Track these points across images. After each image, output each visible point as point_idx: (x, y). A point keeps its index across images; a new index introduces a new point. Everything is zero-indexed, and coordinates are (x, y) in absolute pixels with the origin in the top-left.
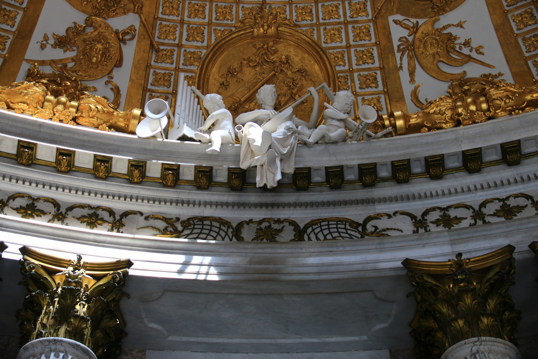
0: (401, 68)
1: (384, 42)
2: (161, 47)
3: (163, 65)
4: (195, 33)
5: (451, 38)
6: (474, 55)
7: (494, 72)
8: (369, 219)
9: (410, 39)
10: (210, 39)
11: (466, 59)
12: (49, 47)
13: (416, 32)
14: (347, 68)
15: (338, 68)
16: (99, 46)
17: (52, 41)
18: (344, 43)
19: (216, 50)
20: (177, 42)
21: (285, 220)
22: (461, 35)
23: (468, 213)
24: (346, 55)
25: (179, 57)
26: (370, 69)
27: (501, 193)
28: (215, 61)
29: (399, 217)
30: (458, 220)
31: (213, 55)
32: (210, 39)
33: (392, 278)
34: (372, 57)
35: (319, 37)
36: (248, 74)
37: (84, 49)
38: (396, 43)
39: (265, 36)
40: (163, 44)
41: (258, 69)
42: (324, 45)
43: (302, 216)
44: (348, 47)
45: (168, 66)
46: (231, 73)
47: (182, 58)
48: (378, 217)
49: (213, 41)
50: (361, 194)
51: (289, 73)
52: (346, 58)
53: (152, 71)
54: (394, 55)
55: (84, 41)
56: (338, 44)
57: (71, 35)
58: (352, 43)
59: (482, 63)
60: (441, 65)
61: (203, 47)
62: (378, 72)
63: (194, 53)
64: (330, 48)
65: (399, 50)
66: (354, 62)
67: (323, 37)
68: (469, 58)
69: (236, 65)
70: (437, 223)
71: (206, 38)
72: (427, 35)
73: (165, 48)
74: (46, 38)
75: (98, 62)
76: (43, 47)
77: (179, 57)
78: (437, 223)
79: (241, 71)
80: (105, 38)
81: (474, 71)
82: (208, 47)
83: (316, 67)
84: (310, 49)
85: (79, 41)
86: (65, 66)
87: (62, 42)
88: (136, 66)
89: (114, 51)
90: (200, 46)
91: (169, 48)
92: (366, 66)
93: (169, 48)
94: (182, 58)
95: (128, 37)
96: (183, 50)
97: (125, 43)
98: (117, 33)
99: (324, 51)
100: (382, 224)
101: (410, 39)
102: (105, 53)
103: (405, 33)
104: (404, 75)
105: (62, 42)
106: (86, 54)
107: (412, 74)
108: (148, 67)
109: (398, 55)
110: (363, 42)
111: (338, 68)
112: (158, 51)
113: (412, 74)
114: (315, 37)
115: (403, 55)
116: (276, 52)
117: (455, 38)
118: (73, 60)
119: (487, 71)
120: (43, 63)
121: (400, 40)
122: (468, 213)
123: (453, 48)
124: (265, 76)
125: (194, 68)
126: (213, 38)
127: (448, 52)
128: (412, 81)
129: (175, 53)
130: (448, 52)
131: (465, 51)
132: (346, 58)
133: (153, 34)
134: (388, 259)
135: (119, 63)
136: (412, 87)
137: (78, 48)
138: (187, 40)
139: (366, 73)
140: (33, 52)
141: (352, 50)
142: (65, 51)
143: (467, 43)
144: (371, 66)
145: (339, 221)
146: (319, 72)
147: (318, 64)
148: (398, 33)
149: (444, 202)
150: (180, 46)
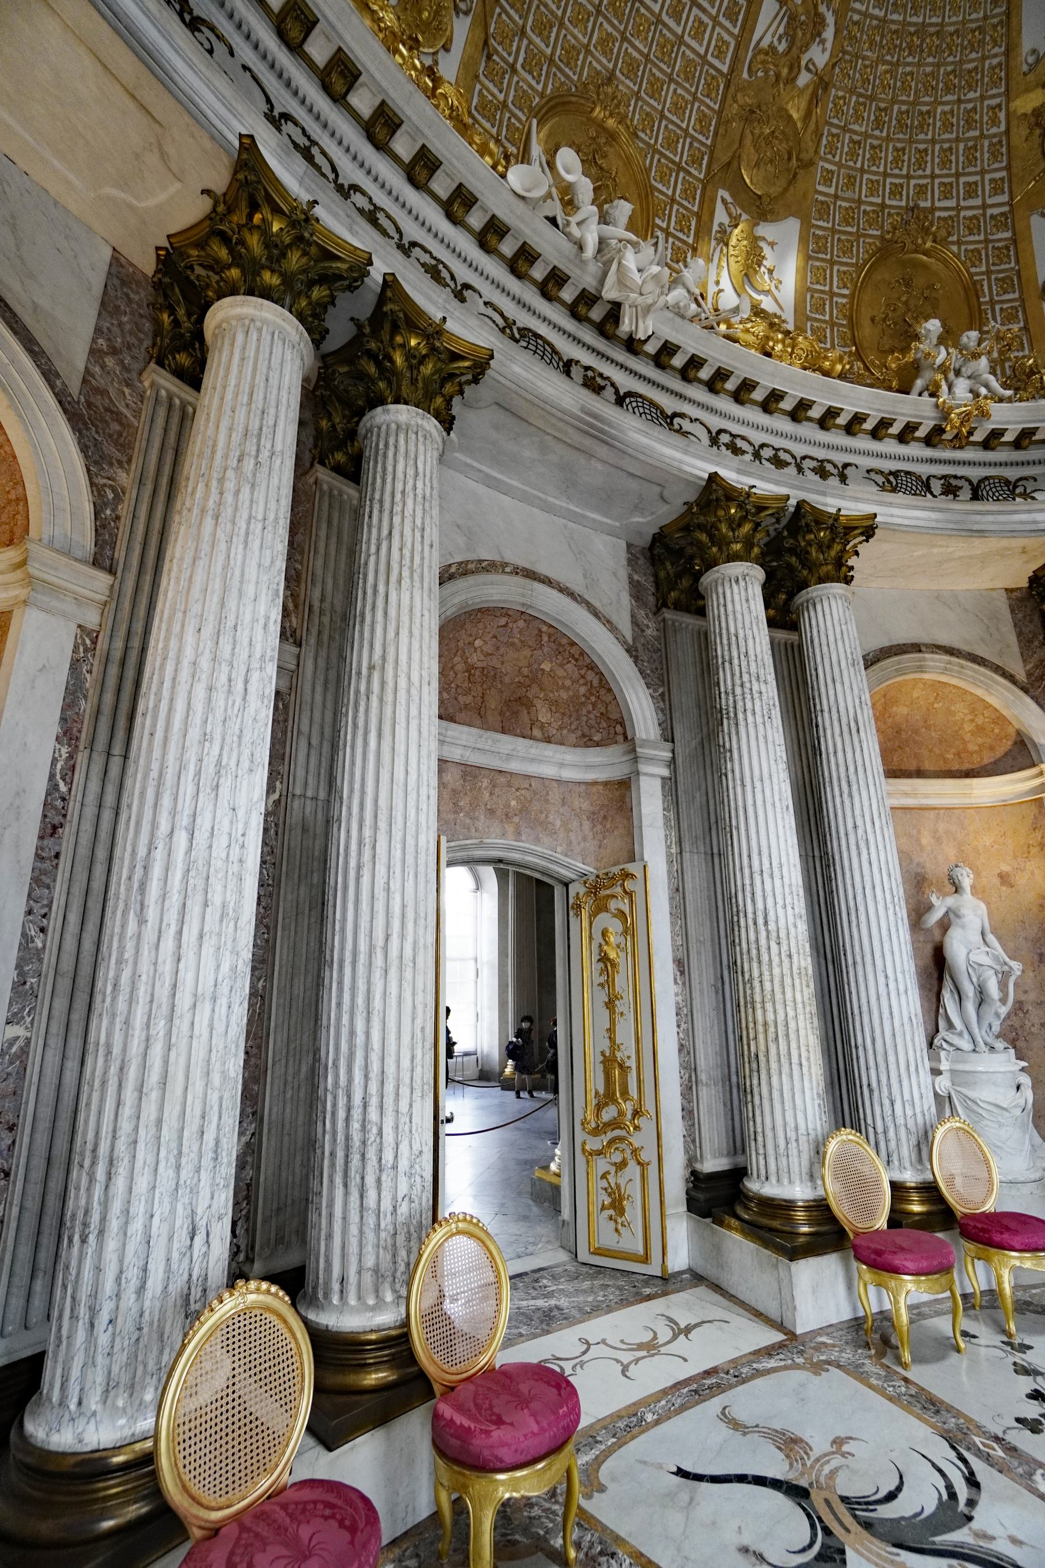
1: (705, 218)
8: (675, 415)
21: (608, 378)
23: (750, 449)
27: (778, 442)
29: (698, 424)
30: (744, 452)
33: (688, 482)
38: (715, 228)
39: (601, 126)
43: (625, 383)
48: (682, 415)
50: (677, 385)
70: (726, 445)
78: (726, 445)
81: (767, 304)
100: (687, 426)
103: (726, 220)
119: (779, 312)
122: (750, 449)
134: (699, 464)
136: (716, 289)
145: (652, 404)
149: (736, 429)
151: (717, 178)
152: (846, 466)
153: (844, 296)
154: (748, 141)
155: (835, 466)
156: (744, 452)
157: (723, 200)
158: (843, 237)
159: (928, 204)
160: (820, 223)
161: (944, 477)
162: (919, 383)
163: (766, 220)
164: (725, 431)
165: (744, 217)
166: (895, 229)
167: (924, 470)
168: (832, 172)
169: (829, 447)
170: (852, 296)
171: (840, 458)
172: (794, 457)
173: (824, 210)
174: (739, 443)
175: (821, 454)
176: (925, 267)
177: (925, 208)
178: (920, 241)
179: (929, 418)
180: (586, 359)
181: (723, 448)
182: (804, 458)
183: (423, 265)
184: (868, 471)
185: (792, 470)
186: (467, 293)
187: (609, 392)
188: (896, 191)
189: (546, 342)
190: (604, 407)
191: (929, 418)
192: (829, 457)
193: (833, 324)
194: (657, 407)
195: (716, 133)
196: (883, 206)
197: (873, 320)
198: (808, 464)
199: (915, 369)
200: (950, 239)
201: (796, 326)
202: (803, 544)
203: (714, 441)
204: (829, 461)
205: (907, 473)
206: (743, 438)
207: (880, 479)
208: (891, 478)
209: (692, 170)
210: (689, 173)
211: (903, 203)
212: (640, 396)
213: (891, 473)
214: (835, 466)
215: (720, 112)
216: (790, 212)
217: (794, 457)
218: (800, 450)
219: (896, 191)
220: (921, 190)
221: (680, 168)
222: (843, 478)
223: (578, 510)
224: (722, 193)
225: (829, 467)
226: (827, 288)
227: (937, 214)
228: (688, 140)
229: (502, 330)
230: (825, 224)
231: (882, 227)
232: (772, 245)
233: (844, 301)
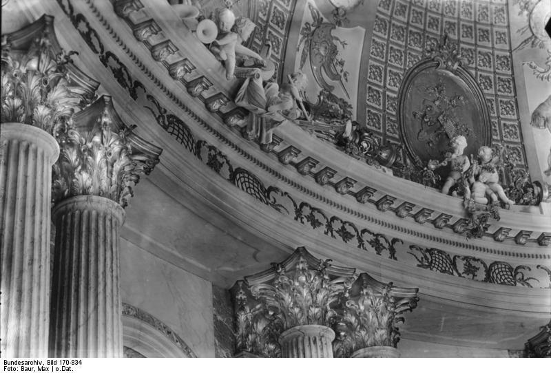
5: (334, 51)
8: (271, 189)
21: (224, 157)
23: (324, 222)
30: (320, 224)
48: (276, 190)
50: (274, 164)
81: (338, 93)
100: (281, 200)
119: (346, 99)
143: (342, 63)
152: (395, 240)
155: (387, 241)
156: (320, 224)
159: (456, 38)
160: (379, 34)
161: (466, 258)
162: (450, 182)
164: (306, 204)
167: (452, 250)
169: (383, 224)
171: (391, 234)
172: (356, 230)
174: (317, 216)
175: (376, 228)
178: (450, 64)
180: (211, 140)
181: (305, 220)
182: (364, 231)
183: (114, 71)
184: (411, 247)
185: (355, 241)
186: (139, 89)
187: (225, 170)
189: (185, 127)
190: (220, 182)
192: (382, 232)
194: (256, 180)
198: (367, 237)
199: (445, 173)
202: (362, 308)
203: (299, 212)
204: (382, 236)
205: (440, 252)
206: (319, 211)
207: (420, 255)
208: (428, 254)
212: (247, 172)
213: (427, 250)
214: (387, 241)
217: (356, 230)
218: (361, 224)
222: (392, 251)
223: (180, 256)
225: (382, 241)
227: (462, 45)
229: (158, 119)
231: (423, 46)
233: (396, 96)
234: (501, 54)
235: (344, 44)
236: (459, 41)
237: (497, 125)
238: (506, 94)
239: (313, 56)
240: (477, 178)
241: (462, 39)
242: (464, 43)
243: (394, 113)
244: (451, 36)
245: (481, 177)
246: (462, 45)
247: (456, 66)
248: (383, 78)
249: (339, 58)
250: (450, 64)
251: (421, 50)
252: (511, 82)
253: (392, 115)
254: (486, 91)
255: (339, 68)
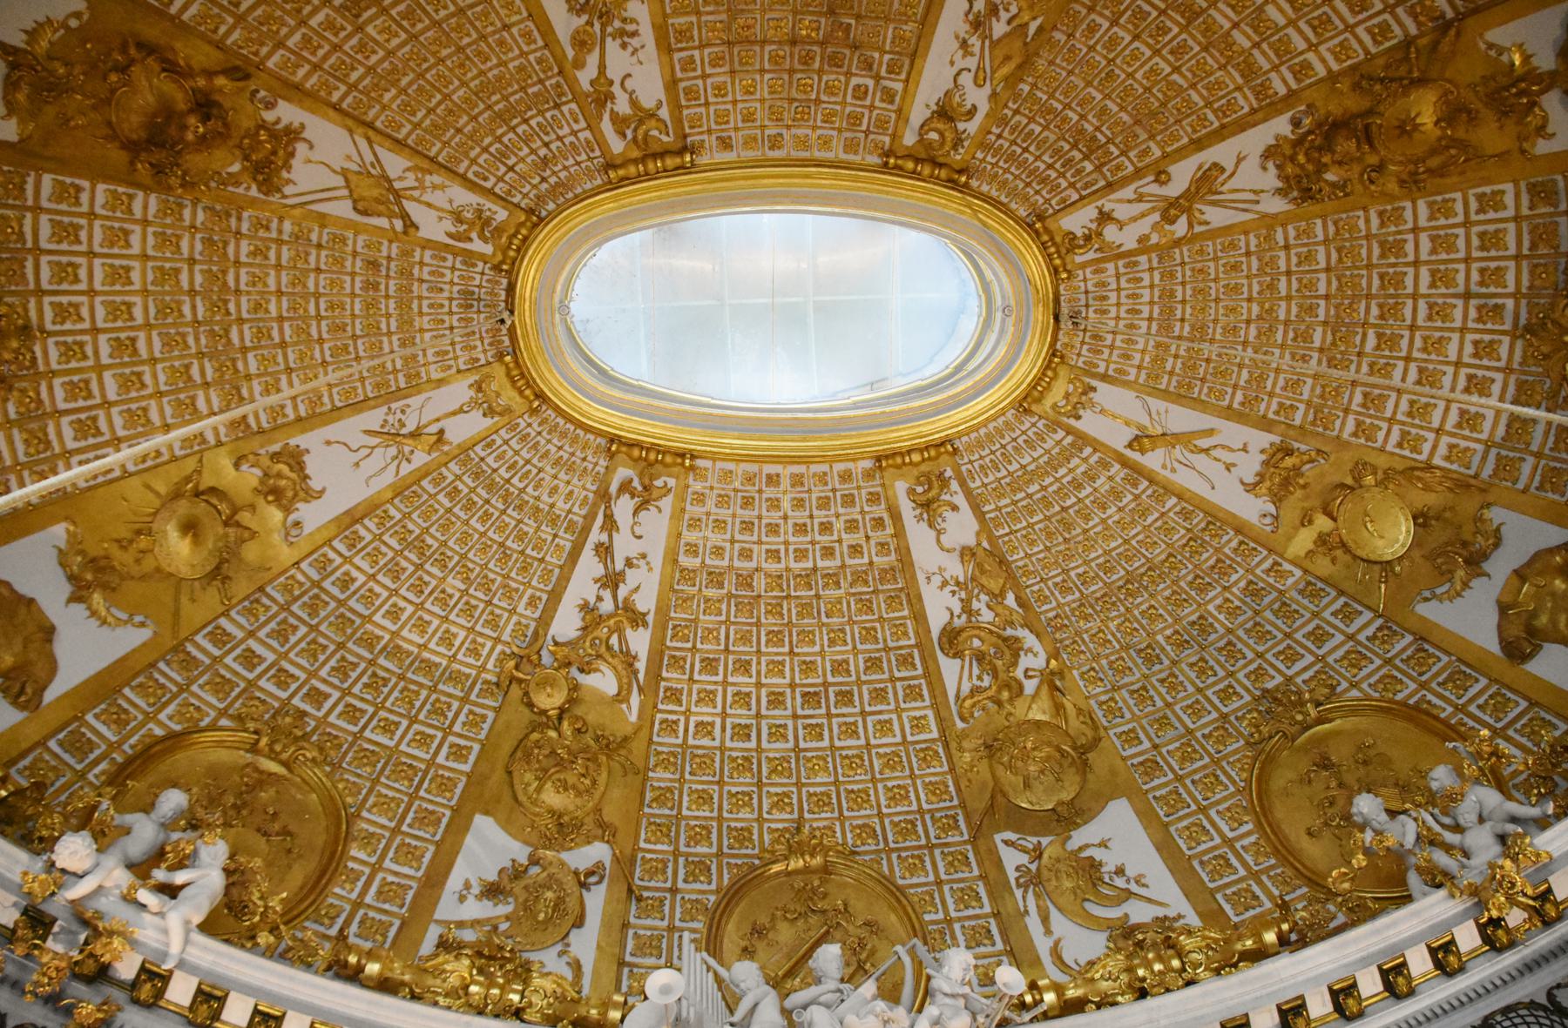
0: (1027, 912)
2: (645, 894)
3: (649, 922)
4: (699, 868)
5: (1094, 865)
6: (1134, 888)
7: (1172, 914)
9: (1033, 867)
10: (720, 876)
11: (1124, 895)
12: (471, 900)
13: (1040, 856)
14: (941, 916)
15: (927, 917)
16: (549, 895)
17: (476, 890)
18: (931, 878)
19: (732, 896)
20: (668, 885)
22: (1109, 860)
24: (936, 895)
25: (673, 908)
26: (977, 917)
28: (730, 917)
31: (728, 904)
32: (720, 876)
34: (978, 899)
35: (891, 869)
36: (785, 933)
37: (526, 900)
38: (1012, 875)
39: (807, 870)
40: (647, 889)
41: (800, 923)
42: (900, 882)
44: (939, 883)
45: (658, 923)
46: (758, 931)
47: (678, 910)
49: (726, 881)
51: (851, 928)
52: (938, 901)
53: (631, 932)
54: (1012, 894)
55: (526, 888)
56: (923, 880)
57: (506, 880)
58: (943, 877)
59: (1149, 900)
60: (1087, 905)
61: (711, 892)
62: (992, 921)
63: (697, 901)
64: (912, 886)
65: (1019, 886)
66: (951, 907)
67: (897, 869)
68: (1129, 894)
69: (763, 920)
71: (714, 877)
72: (1058, 860)
73: (650, 894)
74: (467, 886)
75: (548, 920)
76: (462, 899)
77: (673, 908)
79: (773, 927)
80: (560, 883)
81: (1139, 913)
82: (718, 891)
83: (893, 918)
84: (879, 889)
85: (518, 887)
86: (496, 928)
87: (492, 891)
88: (606, 924)
89: (572, 903)
90: (706, 890)
91: (657, 895)
92: (970, 912)
93: (657, 895)
94: (678, 910)
95: (593, 879)
96: (679, 897)
97: (589, 890)
98: (576, 873)
99: (898, 888)
101: (1033, 867)
102: (559, 903)
103: (1023, 859)
104: (1033, 923)
105: (492, 891)
106: (528, 908)
107: (1045, 920)
108: (626, 925)
109: (1018, 893)
110: (960, 875)
111: (927, 917)
112: (639, 899)
113: (1045, 920)
114: (886, 869)
115: (1026, 891)
116: (825, 895)
117: (1100, 864)
118: (507, 918)
119: (1160, 912)
120: (461, 925)
121: (1018, 869)
123: (1101, 879)
124: (812, 933)
125: (695, 925)
126: (726, 877)
127: (1094, 885)
128: (1048, 932)
129: (667, 902)
130: (1094, 885)
131: (1120, 882)
132: (938, 901)
133: (632, 874)
135: (579, 922)
137: (516, 900)
138: (685, 881)
139: (973, 923)
140: (448, 908)
141: (946, 888)
142: (496, 905)
143: (1120, 871)
144: (978, 911)
146: (898, 925)
147: (894, 910)
148: (1012, 860)
150: (674, 891)
151: (984, 827)
153: (1249, 834)
154: (1000, 771)
157: (1006, 842)
158: (1196, 777)
159: (1279, 679)
160: (1156, 782)
163: (1078, 826)
165: (1045, 841)
166: (1257, 726)
168: (1132, 730)
170: (1259, 825)
173: (1151, 768)
176: (1336, 733)
177: (1277, 687)
178: (1299, 717)
179: (1459, 919)
188: (1226, 694)
191: (1459, 919)
193: (1256, 876)
195: (958, 790)
196: (1224, 717)
197: (1310, 833)
200: (1339, 689)
201: (1201, 915)
209: (950, 840)
210: (946, 845)
211: (1247, 698)
215: (952, 770)
216: (1102, 800)
219: (1226, 694)
220: (1258, 674)
221: (931, 847)
224: (998, 838)
226: (1218, 840)
228: (927, 817)
230: (1163, 780)
232: (1103, 844)
233: (1253, 839)
234: (1370, 631)
235: (1103, 844)
236: (1289, 680)
237: (1466, 720)
238: (1435, 669)
239: (1054, 896)
240: (1458, 828)
241: (1290, 673)
242: (1298, 674)
243: (1273, 861)
244: (1270, 685)
245: (1462, 821)
246: (1299, 680)
247: (1313, 712)
248: (1212, 831)
249: (1109, 867)
250: (1299, 717)
251: (1242, 742)
252: (1426, 646)
253: (1272, 867)
254: (1399, 697)
255: (1120, 882)
